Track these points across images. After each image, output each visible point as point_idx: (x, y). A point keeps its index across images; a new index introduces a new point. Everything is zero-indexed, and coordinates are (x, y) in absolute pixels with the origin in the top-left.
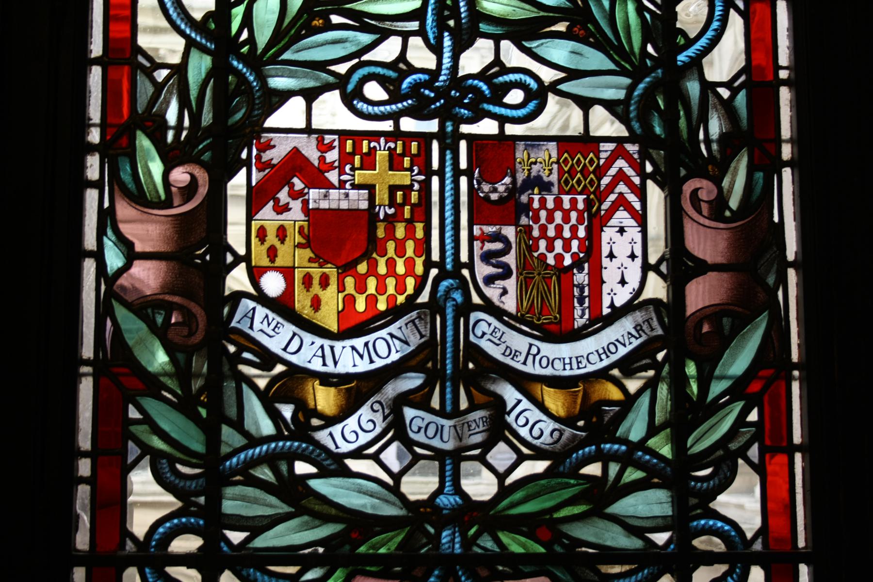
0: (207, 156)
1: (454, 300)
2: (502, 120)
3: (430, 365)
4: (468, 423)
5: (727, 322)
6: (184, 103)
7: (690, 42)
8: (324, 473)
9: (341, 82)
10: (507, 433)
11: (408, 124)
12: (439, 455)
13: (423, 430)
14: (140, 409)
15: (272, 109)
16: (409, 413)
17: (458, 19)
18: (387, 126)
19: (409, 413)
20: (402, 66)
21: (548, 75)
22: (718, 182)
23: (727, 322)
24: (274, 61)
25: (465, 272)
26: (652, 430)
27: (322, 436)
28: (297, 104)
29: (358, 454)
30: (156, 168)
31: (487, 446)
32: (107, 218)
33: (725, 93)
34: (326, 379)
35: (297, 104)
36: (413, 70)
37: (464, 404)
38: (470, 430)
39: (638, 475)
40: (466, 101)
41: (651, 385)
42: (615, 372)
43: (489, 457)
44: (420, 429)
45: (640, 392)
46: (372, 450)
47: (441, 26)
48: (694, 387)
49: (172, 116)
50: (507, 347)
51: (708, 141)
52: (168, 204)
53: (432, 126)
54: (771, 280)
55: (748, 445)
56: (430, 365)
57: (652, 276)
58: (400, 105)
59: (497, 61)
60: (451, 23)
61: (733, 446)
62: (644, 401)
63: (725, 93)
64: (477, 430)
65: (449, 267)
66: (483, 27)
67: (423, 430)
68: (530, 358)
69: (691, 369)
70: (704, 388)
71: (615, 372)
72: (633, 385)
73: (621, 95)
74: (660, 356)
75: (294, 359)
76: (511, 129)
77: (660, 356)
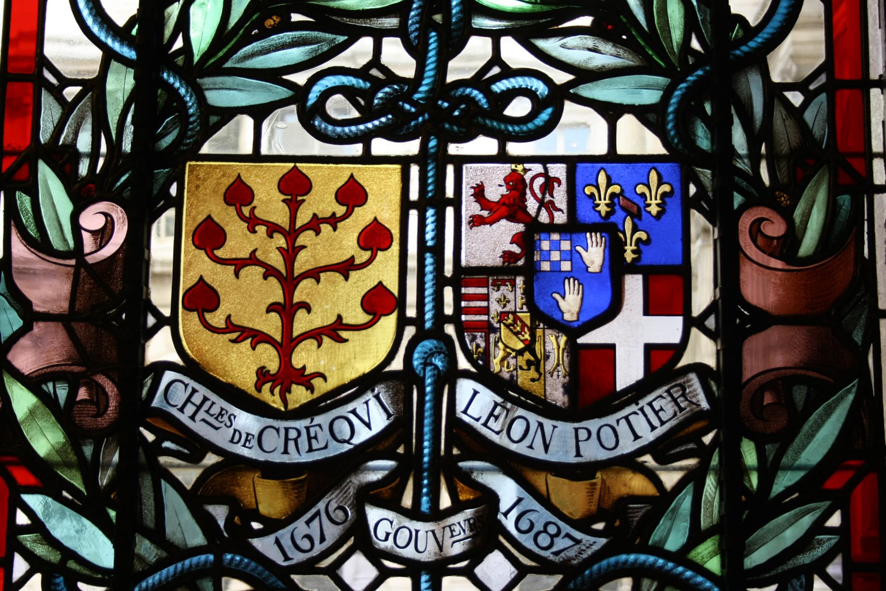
0: (127, 194)
1: (436, 367)
2: (503, 139)
3: (401, 450)
4: (450, 526)
5: (800, 394)
6: (100, 125)
9: (299, 94)
10: (502, 539)
12: (412, 569)
13: (391, 537)
15: (208, 132)
16: (373, 514)
17: (447, 15)
19: (373, 514)
20: (374, 72)
21: (560, 77)
23: (800, 394)
25: (450, 329)
26: (696, 536)
27: (265, 545)
30: (64, 206)
33: (796, 98)
37: (445, 501)
38: (452, 536)
40: (456, 113)
42: (648, 460)
43: (479, 571)
44: (388, 534)
45: (679, 486)
46: (325, 563)
47: (426, 25)
48: (754, 479)
49: (84, 143)
50: (235, 431)
53: (412, 147)
54: (858, 337)
55: (827, 559)
56: (401, 450)
58: (376, 123)
60: (438, 18)
61: (806, 558)
63: (796, 98)
64: (462, 536)
67: (391, 537)
68: (291, 444)
69: (750, 456)
70: (767, 479)
72: (670, 479)
74: (707, 439)
77: (707, 439)
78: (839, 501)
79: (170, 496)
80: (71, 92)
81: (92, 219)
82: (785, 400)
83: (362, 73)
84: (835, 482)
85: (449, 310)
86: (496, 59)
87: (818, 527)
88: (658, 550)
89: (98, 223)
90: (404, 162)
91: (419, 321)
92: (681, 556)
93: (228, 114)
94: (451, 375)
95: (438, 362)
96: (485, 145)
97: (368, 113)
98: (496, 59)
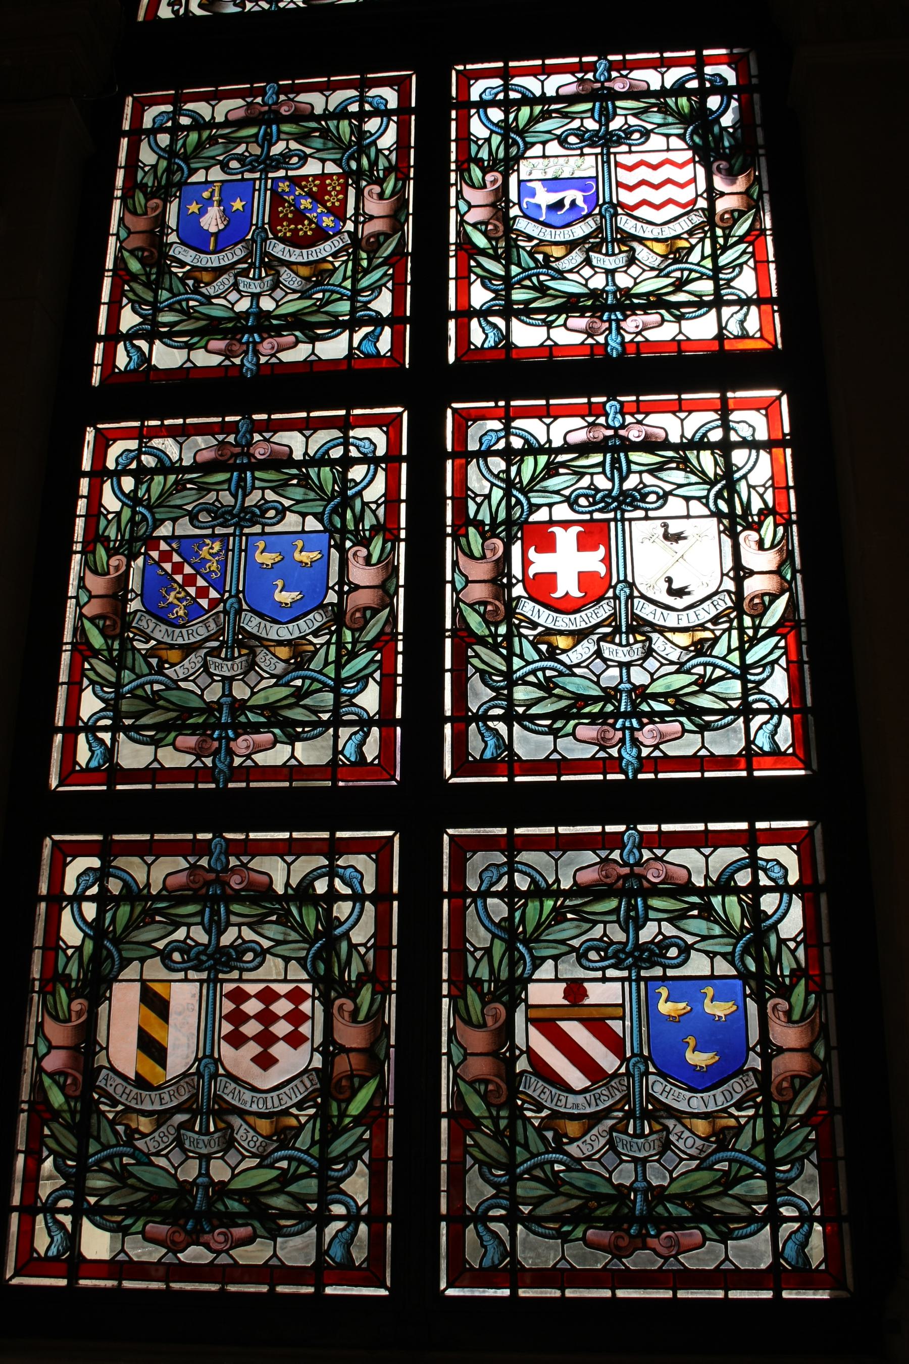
7: (357, 484)
8: (168, 688)
9: (189, 513)
11: (219, 530)
12: (224, 679)
14: (90, 664)
18: (209, 531)
21: (287, 503)
22: (367, 547)
24: (159, 506)
25: (241, 595)
26: (326, 664)
29: (185, 680)
31: (246, 673)
32: (81, 579)
33: (374, 506)
34: (172, 647)
36: (223, 506)
37: (236, 655)
41: (328, 643)
42: (310, 637)
47: (238, 486)
51: (364, 530)
52: (108, 573)
53: (231, 530)
62: (322, 652)
65: (233, 593)
66: (258, 484)
71: (310, 637)
73: (320, 509)
76: (268, 529)
80: (110, 517)
81: (114, 562)
82: (364, 616)
83: (213, 504)
85: (241, 588)
86: (263, 498)
87: (372, 661)
89: (116, 563)
90: (228, 535)
91: (230, 591)
92: (320, 672)
94: (239, 611)
95: (236, 606)
96: (257, 529)
97: (214, 519)
98: (263, 498)
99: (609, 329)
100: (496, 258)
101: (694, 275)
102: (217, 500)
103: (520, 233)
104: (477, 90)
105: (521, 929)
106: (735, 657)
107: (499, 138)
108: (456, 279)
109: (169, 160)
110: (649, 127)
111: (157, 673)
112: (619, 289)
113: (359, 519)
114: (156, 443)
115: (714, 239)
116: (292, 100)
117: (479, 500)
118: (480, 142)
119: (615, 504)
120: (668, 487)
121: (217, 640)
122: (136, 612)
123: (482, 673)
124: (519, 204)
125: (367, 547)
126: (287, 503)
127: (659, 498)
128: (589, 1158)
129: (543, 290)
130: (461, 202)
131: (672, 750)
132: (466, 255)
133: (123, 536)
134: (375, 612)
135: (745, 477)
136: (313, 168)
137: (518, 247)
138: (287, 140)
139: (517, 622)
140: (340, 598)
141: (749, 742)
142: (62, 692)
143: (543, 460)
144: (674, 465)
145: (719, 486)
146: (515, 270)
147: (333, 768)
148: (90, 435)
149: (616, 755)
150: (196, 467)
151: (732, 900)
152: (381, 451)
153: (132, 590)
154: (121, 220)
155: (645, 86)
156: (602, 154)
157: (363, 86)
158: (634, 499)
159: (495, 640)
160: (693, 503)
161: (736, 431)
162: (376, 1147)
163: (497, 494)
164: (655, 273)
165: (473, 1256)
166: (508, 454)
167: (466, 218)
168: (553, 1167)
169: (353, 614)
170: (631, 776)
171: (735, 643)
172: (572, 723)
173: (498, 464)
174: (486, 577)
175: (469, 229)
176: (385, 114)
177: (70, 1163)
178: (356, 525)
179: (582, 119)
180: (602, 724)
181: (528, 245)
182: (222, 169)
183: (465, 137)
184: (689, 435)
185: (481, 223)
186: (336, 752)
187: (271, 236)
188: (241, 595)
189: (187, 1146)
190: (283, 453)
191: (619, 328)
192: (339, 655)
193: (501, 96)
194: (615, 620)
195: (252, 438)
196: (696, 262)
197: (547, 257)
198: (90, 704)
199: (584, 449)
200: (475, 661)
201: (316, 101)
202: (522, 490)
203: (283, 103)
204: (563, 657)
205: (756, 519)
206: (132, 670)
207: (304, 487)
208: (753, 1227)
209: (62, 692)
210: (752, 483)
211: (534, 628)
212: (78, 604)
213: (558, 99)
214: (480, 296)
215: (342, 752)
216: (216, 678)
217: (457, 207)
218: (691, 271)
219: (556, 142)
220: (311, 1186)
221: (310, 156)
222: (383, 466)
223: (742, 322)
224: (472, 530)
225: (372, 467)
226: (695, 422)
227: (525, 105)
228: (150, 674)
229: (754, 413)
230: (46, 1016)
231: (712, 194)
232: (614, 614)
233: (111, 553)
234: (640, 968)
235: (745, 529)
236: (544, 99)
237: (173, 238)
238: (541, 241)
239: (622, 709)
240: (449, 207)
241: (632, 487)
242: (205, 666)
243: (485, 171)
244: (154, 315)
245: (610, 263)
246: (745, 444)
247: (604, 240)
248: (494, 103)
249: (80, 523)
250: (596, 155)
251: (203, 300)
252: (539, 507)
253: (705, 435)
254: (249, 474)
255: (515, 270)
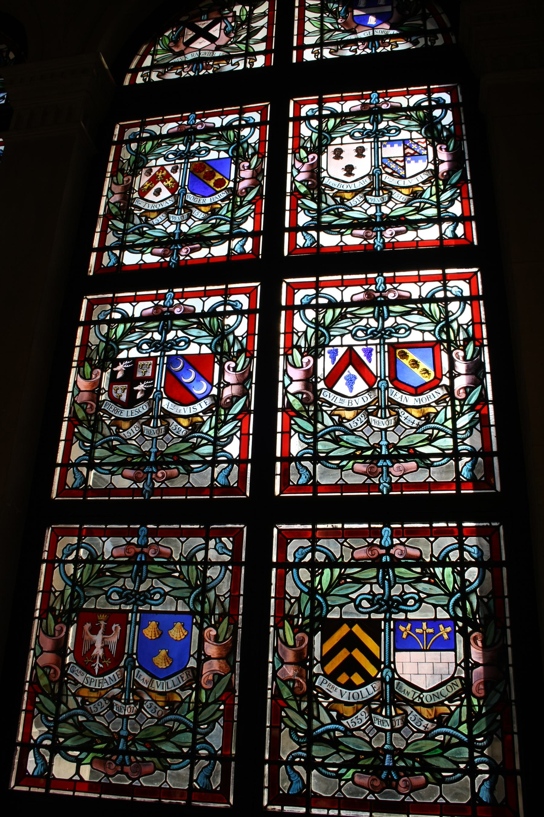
6: (98, 354)
11: (153, 354)
14: (78, 429)
15: (119, 353)
18: (147, 355)
21: (191, 338)
25: (162, 390)
27: (122, 434)
28: (126, 351)
32: (75, 382)
35: (126, 351)
39: (206, 442)
42: (201, 414)
51: (234, 352)
53: (158, 354)
57: (214, 388)
59: (176, 335)
63: (240, 339)
65: (158, 389)
71: (201, 414)
73: (210, 341)
75: (117, 415)
78: (240, 420)
79: (105, 426)
84: (240, 417)
87: (236, 426)
88: (202, 433)
90: (157, 357)
91: (157, 388)
92: (206, 434)
93: (123, 350)
97: (150, 348)
99: (376, 236)
100: (313, 200)
101: (427, 205)
102: (152, 337)
103: (327, 186)
104: (305, 111)
105: (319, 587)
106: (449, 424)
107: (317, 135)
108: (290, 210)
109: (136, 156)
110: (401, 127)
111: (115, 435)
112: (383, 214)
113: (231, 346)
114: (120, 306)
115: (437, 186)
116: (204, 122)
117: (300, 334)
118: (306, 138)
119: (379, 335)
120: (411, 325)
121: (148, 415)
122: (104, 400)
123: (299, 433)
124: (327, 170)
125: (235, 362)
126: (191, 338)
127: (406, 331)
128: (358, 729)
129: (340, 216)
130: (294, 170)
131: (410, 478)
132: (295, 199)
133: (100, 358)
134: (239, 398)
135: (456, 319)
136: (213, 155)
137: (326, 194)
138: (199, 142)
139: (320, 403)
140: (219, 391)
141: (458, 473)
142: (62, 445)
143: (338, 311)
144: (416, 312)
145: (441, 324)
146: (324, 205)
147: (212, 489)
148: (85, 303)
149: (378, 482)
150: (142, 318)
151: (449, 570)
152: (246, 307)
153: (103, 388)
154: (109, 189)
155: (399, 105)
156: (374, 142)
157: (241, 112)
158: (391, 332)
159: (308, 414)
160: (426, 334)
161: (451, 291)
162: (227, 714)
163: (310, 331)
164: (403, 205)
165: (284, 785)
166: (317, 307)
167: (296, 178)
168: (334, 734)
169: (226, 400)
170: (385, 493)
171: (449, 415)
172: (351, 463)
173: (311, 314)
174: (302, 378)
175: (298, 184)
176: (253, 125)
177: (49, 718)
178: (230, 349)
179: (364, 123)
180: (370, 463)
181: (331, 193)
182: (165, 159)
183: (297, 135)
184: (424, 295)
185: (305, 180)
186: (213, 479)
187: (188, 191)
188: (162, 390)
189: (115, 710)
190: (189, 310)
191: (382, 236)
192: (217, 423)
193: (317, 113)
194: (378, 402)
195: (173, 302)
196: (427, 197)
197: (342, 199)
198: (77, 452)
199: (361, 304)
200: (295, 427)
201: (217, 122)
202: (324, 327)
203: (198, 124)
204: (347, 425)
205: (462, 343)
206: (101, 433)
207: (201, 329)
208: (459, 775)
209: (62, 445)
210: (460, 323)
211: (331, 407)
212: (73, 395)
213: (351, 113)
214: (303, 219)
215: (216, 480)
216: (147, 438)
217: (292, 173)
218: (426, 203)
219: (348, 136)
220: (187, 738)
221: (212, 149)
222: (246, 316)
223: (454, 231)
224: (295, 351)
225: (240, 317)
226: (427, 288)
227: (332, 118)
228: (111, 435)
229: (462, 282)
230: (41, 632)
231: (437, 162)
232: (378, 398)
233: (93, 367)
234: (392, 613)
235: (455, 349)
236: (343, 114)
237: (136, 195)
238: (339, 190)
239: (383, 453)
240: (286, 173)
241: (390, 325)
242: (142, 431)
243: (308, 153)
244: (123, 237)
245: (378, 200)
246: (456, 298)
247: (374, 189)
248: (313, 117)
249: (77, 351)
250: (371, 142)
251: (151, 227)
252: (335, 336)
253: (433, 295)
254: (169, 322)
255: (324, 205)
